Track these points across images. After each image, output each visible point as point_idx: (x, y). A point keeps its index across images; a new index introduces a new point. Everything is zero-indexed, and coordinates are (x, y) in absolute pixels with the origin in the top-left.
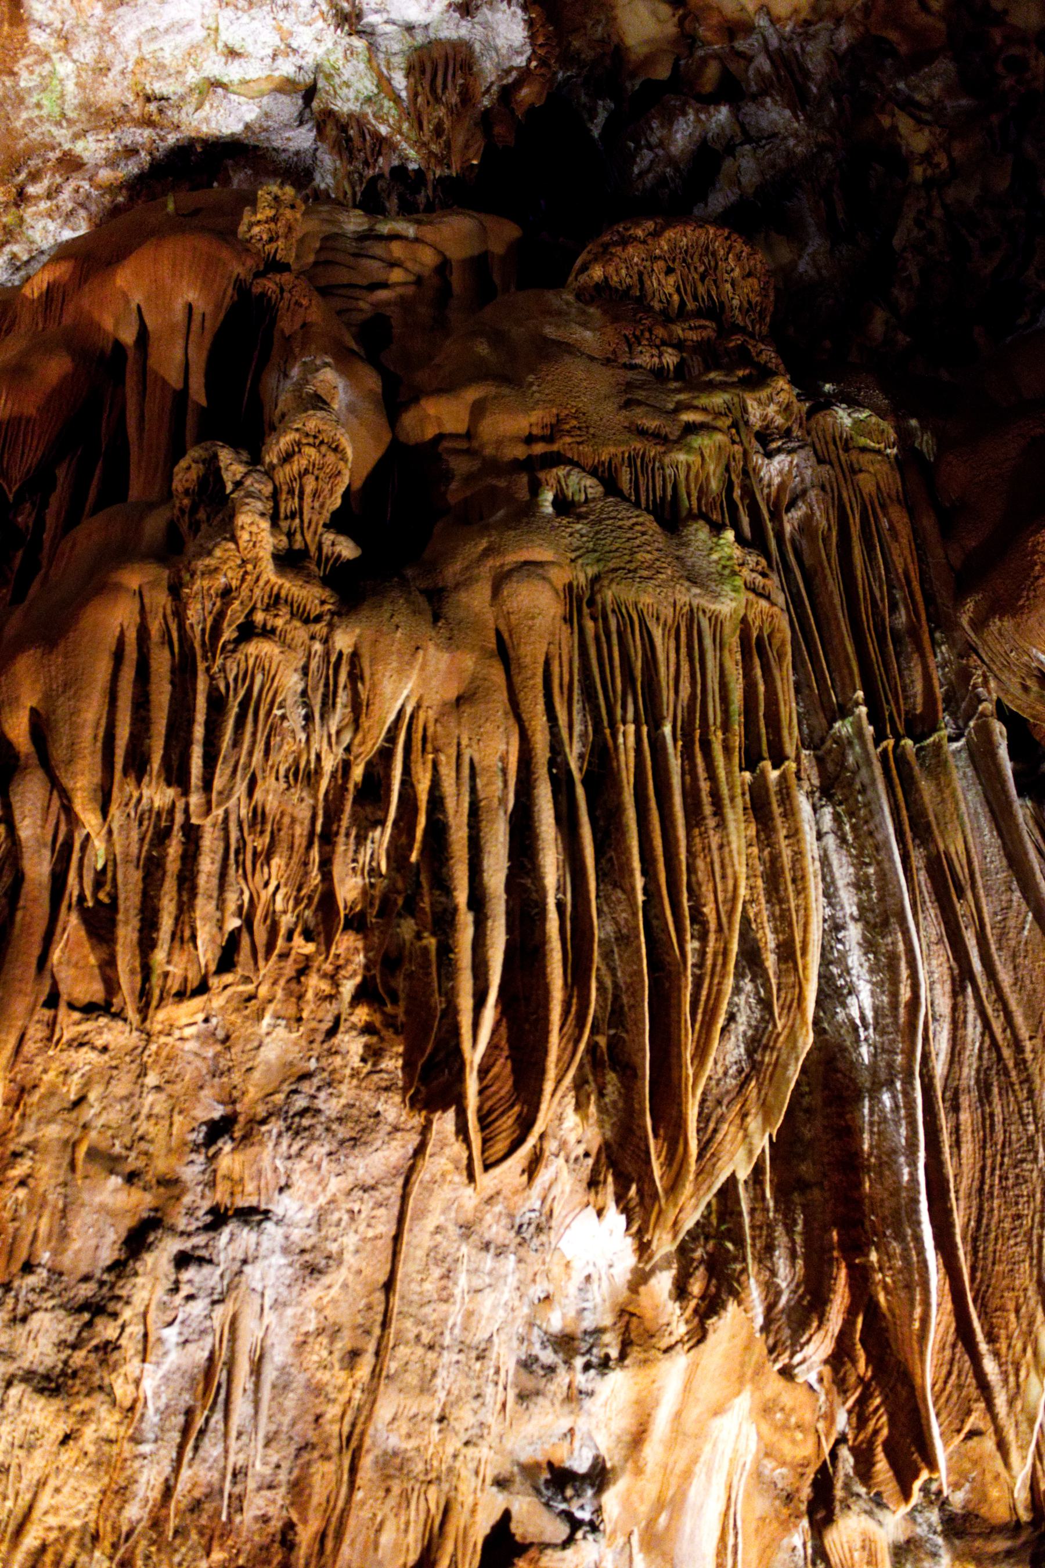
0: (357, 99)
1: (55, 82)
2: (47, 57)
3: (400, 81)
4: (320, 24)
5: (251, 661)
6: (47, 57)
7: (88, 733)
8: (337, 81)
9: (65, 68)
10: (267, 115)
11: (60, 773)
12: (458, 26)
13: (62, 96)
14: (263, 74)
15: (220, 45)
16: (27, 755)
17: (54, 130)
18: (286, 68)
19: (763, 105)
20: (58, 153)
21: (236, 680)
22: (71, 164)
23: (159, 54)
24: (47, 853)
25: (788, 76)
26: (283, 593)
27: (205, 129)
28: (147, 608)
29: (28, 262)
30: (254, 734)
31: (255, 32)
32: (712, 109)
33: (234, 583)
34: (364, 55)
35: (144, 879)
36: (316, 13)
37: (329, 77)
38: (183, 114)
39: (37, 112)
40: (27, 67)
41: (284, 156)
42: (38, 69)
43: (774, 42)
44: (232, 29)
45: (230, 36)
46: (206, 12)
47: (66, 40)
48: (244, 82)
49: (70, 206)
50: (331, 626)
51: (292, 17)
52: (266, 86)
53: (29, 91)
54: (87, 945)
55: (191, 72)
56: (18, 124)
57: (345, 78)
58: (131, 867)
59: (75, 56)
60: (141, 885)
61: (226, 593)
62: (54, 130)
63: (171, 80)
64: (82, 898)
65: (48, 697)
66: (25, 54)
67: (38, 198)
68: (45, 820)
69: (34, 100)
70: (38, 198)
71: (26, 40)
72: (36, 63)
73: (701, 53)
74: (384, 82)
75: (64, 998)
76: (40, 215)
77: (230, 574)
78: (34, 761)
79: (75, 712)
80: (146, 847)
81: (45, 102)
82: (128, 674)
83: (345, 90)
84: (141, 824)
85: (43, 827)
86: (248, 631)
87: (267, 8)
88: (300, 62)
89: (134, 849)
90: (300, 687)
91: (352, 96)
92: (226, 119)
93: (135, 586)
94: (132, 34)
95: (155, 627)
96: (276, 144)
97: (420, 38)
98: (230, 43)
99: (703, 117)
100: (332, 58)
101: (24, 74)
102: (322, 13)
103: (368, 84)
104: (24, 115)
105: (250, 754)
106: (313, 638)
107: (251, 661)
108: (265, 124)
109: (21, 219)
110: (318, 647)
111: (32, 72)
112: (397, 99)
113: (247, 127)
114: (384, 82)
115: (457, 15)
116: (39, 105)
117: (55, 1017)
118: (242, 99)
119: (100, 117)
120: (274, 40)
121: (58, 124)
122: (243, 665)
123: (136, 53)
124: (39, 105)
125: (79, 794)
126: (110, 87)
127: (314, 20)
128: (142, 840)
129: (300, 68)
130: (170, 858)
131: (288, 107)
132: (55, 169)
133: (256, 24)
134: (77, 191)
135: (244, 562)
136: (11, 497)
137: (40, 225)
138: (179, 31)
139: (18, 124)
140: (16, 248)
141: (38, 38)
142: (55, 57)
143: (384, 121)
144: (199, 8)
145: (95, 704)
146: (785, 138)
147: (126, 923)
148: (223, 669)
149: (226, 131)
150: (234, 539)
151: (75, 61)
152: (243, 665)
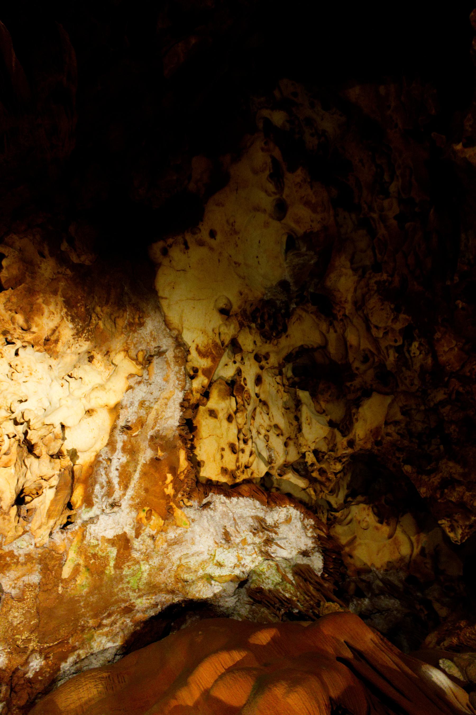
0: (273, 584)
1: (140, 573)
2: (138, 563)
3: (290, 576)
4: (254, 556)
6: (138, 563)
8: (263, 576)
9: (145, 567)
10: (224, 590)
12: (302, 560)
13: (140, 579)
14: (228, 573)
15: (215, 561)
17: (131, 594)
18: (237, 572)
19: (380, 598)
20: (127, 604)
22: (129, 610)
23: (189, 564)
25: (389, 589)
27: (197, 595)
29: (83, 659)
31: (228, 557)
32: (362, 599)
34: (275, 567)
36: (254, 552)
37: (259, 575)
38: (191, 589)
39: (126, 585)
40: (128, 566)
41: (221, 609)
42: (132, 567)
43: (380, 576)
44: (221, 555)
45: (219, 558)
46: (210, 549)
47: (148, 557)
48: (220, 577)
49: (118, 630)
51: (244, 553)
52: (228, 579)
53: (126, 576)
55: (201, 571)
56: (116, 590)
57: (267, 575)
59: (150, 563)
62: (131, 594)
63: (191, 574)
66: (128, 561)
67: (106, 626)
69: (127, 580)
70: (106, 626)
71: (130, 555)
72: (133, 565)
73: (348, 580)
74: (284, 578)
76: (103, 634)
81: (132, 581)
83: (267, 580)
87: (235, 549)
88: (244, 570)
91: (270, 582)
92: (204, 592)
94: (177, 556)
96: (220, 604)
97: (293, 563)
98: (219, 560)
99: (359, 602)
100: (261, 568)
101: (126, 569)
102: (256, 552)
103: (277, 578)
104: (120, 586)
108: (222, 594)
109: (93, 636)
111: (129, 568)
112: (292, 584)
113: (215, 595)
114: (284, 578)
115: (301, 556)
116: (128, 582)
118: (217, 583)
119: (153, 588)
120: (235, 561)
121: (134, 591)
123: (178, 563)
124: (128, 582)
126: (162, 576)
127: (253, 554)
129: (243, 572)
131: (232, 587)
132: (119, 613)
133: (230, 555)
134: (123, 623)
137: (98, 640)
138: (198, 556)
139: (116, 590)
140: (81, 652)
141: (135, 555)
142: (142, 563)
143: (288, 592)
144: (207, 548)
146: (392, 611)
149: (205, 597)
151: (150, 565)
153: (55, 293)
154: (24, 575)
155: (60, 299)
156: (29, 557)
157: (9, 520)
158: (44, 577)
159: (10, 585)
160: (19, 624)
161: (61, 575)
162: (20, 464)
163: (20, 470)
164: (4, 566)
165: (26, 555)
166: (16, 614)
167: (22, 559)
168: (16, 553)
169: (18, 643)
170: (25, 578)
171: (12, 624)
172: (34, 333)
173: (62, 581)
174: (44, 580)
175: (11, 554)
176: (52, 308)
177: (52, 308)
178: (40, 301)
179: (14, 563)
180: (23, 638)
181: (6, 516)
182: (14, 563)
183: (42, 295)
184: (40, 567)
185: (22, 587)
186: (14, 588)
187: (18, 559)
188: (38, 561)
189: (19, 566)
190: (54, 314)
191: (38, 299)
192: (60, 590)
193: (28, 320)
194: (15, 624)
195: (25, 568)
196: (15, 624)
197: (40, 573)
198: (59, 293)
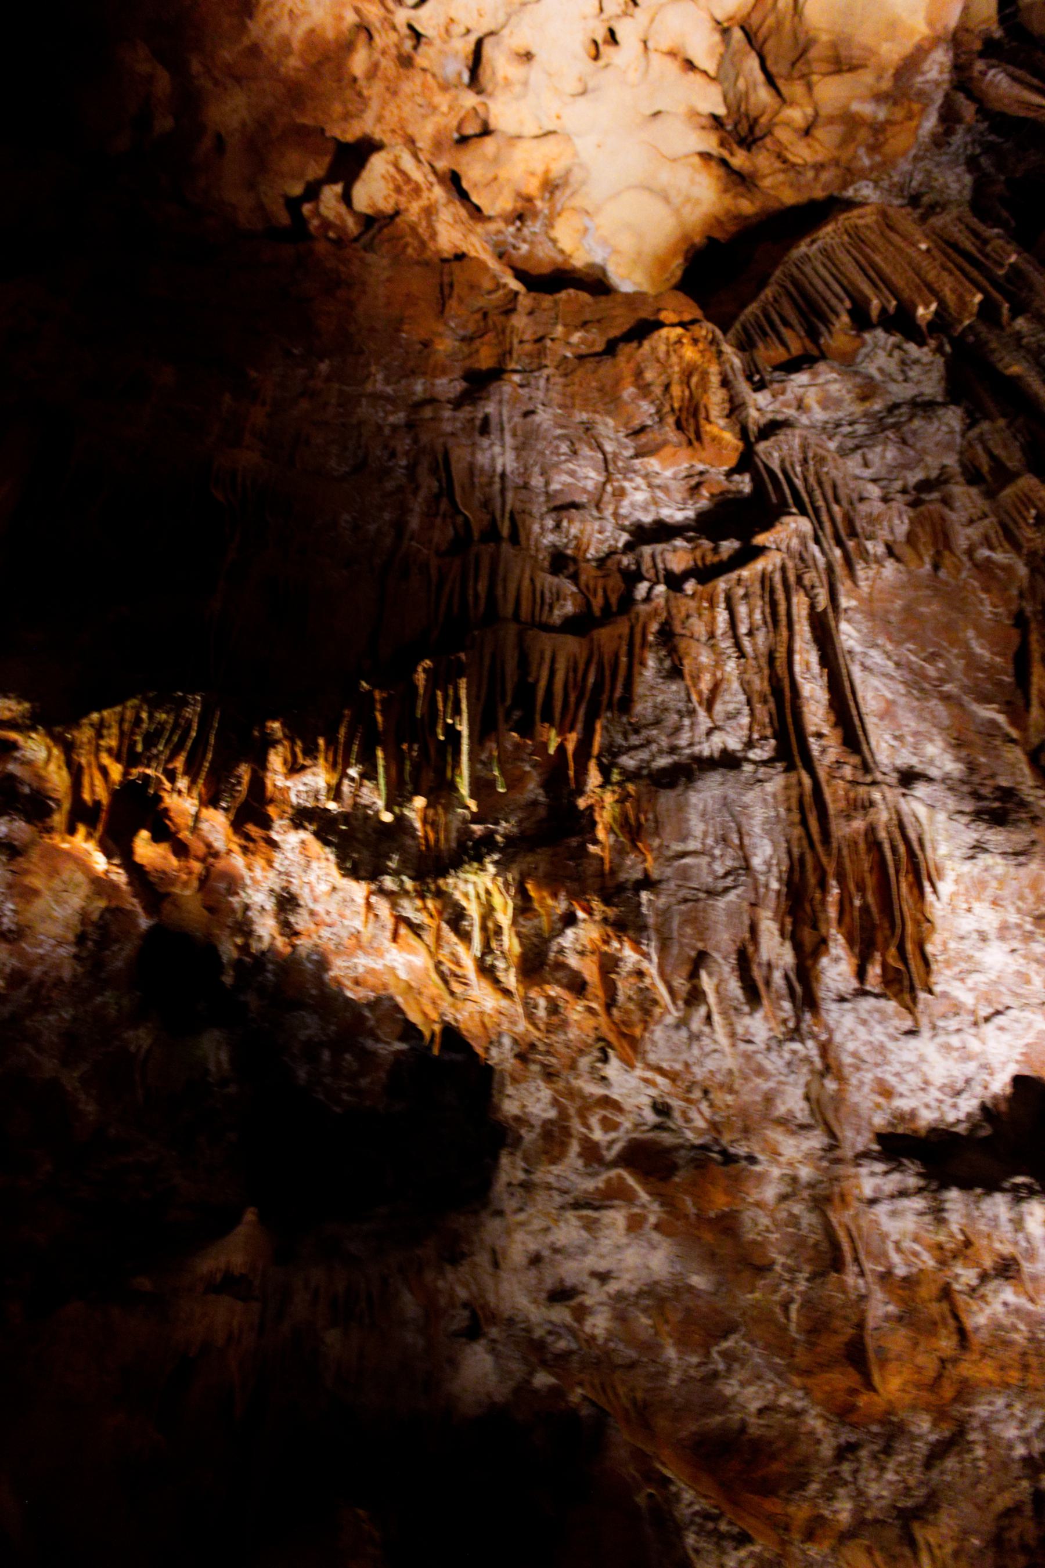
153: (255, 51)
155: (255, 28)
172: (357, 11)
176: (284, 27)
177: (284, 27)
178: (293, 62)
183: (283, 70)
190: (291, 11)
191: (297, 70)
193: (348, 47)
198: (246, 42)
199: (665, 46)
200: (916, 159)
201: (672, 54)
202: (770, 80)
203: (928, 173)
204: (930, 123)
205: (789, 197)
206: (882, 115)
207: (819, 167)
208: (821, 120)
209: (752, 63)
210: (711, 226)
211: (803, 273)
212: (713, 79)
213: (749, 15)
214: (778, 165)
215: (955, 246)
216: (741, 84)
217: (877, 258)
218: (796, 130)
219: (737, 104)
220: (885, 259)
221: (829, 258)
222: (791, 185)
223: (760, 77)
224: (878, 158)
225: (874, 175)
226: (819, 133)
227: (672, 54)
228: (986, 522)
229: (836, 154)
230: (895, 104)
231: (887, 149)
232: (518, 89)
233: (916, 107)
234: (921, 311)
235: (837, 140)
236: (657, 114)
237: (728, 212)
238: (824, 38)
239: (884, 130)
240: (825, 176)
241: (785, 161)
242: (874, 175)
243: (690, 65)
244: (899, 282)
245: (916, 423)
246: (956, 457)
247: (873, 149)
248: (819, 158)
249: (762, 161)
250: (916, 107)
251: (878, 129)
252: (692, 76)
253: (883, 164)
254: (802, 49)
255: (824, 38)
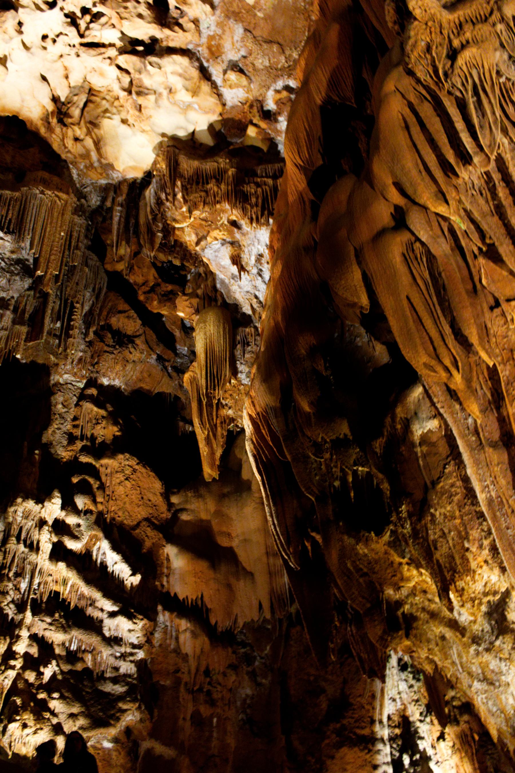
5: (464, 68)
7: (414, 172)
11: (417, 200)
16: (405, 205)
21: (463, 85)
24: (442, 240)
26: (462, 19)
28: (403, 92)
30: (490, 102)
33: (428, 40)
35: (500, 218)
50: (499, 9)
54: (497, 268)
58: (489, 219)
60: (501, 222)
61: (428, 49)
64: (480, 249)
65: (393, 174)
68: (431, 227)
75: (502, 300)
77: (423, 38)
78: (410, 204)
79: (403, 168)
80: (491, 203)
82: (415, 130)
84: (481, 194)
85: (432, 230)
86: (453, 55)
89: (486, 208)
90: (506, 57)
93: (393, 88)
95: (412, 98)
105: (494, 113)
106: (494, 25)
107: (464, 68)
110: (500, 27)
117: (502, 310)
122: (462, 74)
125: (428, 202)
128: (487, 201)
130: (503, 199)
135: (426, 24)
136: (355, 106)
145: (409, 157)
147: (501, 244)
148: (453, 86)
150: (415, 19)
152: (462, 74)
154: (233, 38)
156: (219, 24)
157: (175, 37)
158: (242, 22)
159: (236, 53)
160: (269, 61)
161: (248, 4)
162: (122, 10)
163: (129, 13)
164: (218, 49)
165: (217, 26)
166: (260, 61)
167: (219, 32)
168: (212, 33)
169: (286, 65)
170: (236, 38)
171: (266, 67)
173: (254, 7)
174: (244, 24)
175: (211, 38)
179: (219, 39)
180: (284, 61)
181: (171, 38)
182: (219, 39)
184: (232, 20)
185: (242, 44)
186: (239, 50)
187: (218, 35)
188: (227, 19)
189: (224, 37)
192: (260, 14)
194: (267, 64)
195: (228, 33)
196: (267, 64)
197: (237, 24)
199: (66, 64)
200: (92, 183)
201: (66, 68)
202: (83, 110)
203: (91, 192)
204: (103, 182)
205: (55, 147)
206: (96, 164)
207: (69, 152)
208: (81, 142)
209: (83, 98)
210: (28, 120)
211: (30, 202)
212: (70, 87)
213: (95, 90)
214: (61, 137)
215: (71, 236)
216: (75, 98)
217: (48, 229)
218: (74, 135)
219: (69, 102)
220: (50, 231)
221: (40, 206)
222: (59, 145)
223: (81, 105)
224: (85, 171)
225: (80, 173)
226: (79, 145)
227: (66, 68)
228: (5, 332)
229: (77, 156)
230: (101, 167)
231: (89, 172)
232: (7, 37)
233: (104, 175)
234: (39, 272)
235: (80, 153)
236: (44, 78)
237: (36, 124)
238: (102, 132)
239: (92, 168)
240: (69, 155)
241: (63, 139)
242: (80, 173)
243: (67, 77)
244: (43, 253)
245: (17, 278)
246: (18, 295)
247: (86, 167)
248: (72, 151)
249: (58, 130)
250: (104, 175)
251: (92, 165)
252: (65, 80)
253: (85, 174)
254: (94, 124)
255: (102, 132)
